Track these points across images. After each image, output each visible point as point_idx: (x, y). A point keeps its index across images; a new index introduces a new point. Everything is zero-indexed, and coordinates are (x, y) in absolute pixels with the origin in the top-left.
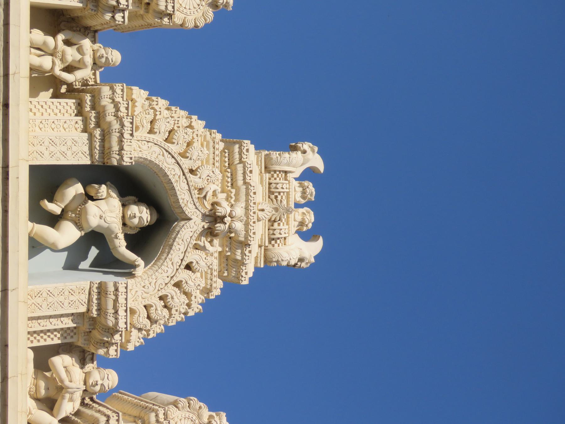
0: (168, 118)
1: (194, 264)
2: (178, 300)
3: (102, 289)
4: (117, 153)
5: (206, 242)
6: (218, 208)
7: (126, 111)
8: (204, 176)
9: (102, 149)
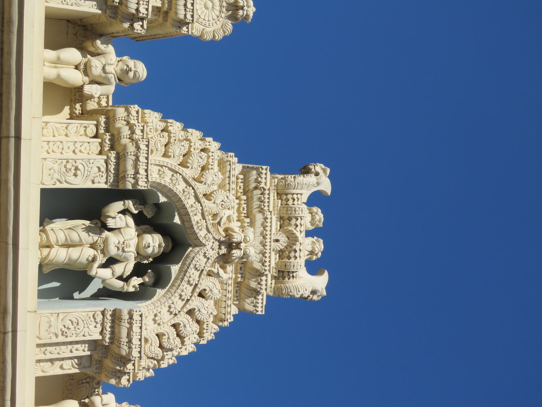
1: (207, 292)
3: (116, 316)
4: (132, 176)
5: (219, 269)
6: (234, 234)
7: (142, 134)
9: (116, 172)
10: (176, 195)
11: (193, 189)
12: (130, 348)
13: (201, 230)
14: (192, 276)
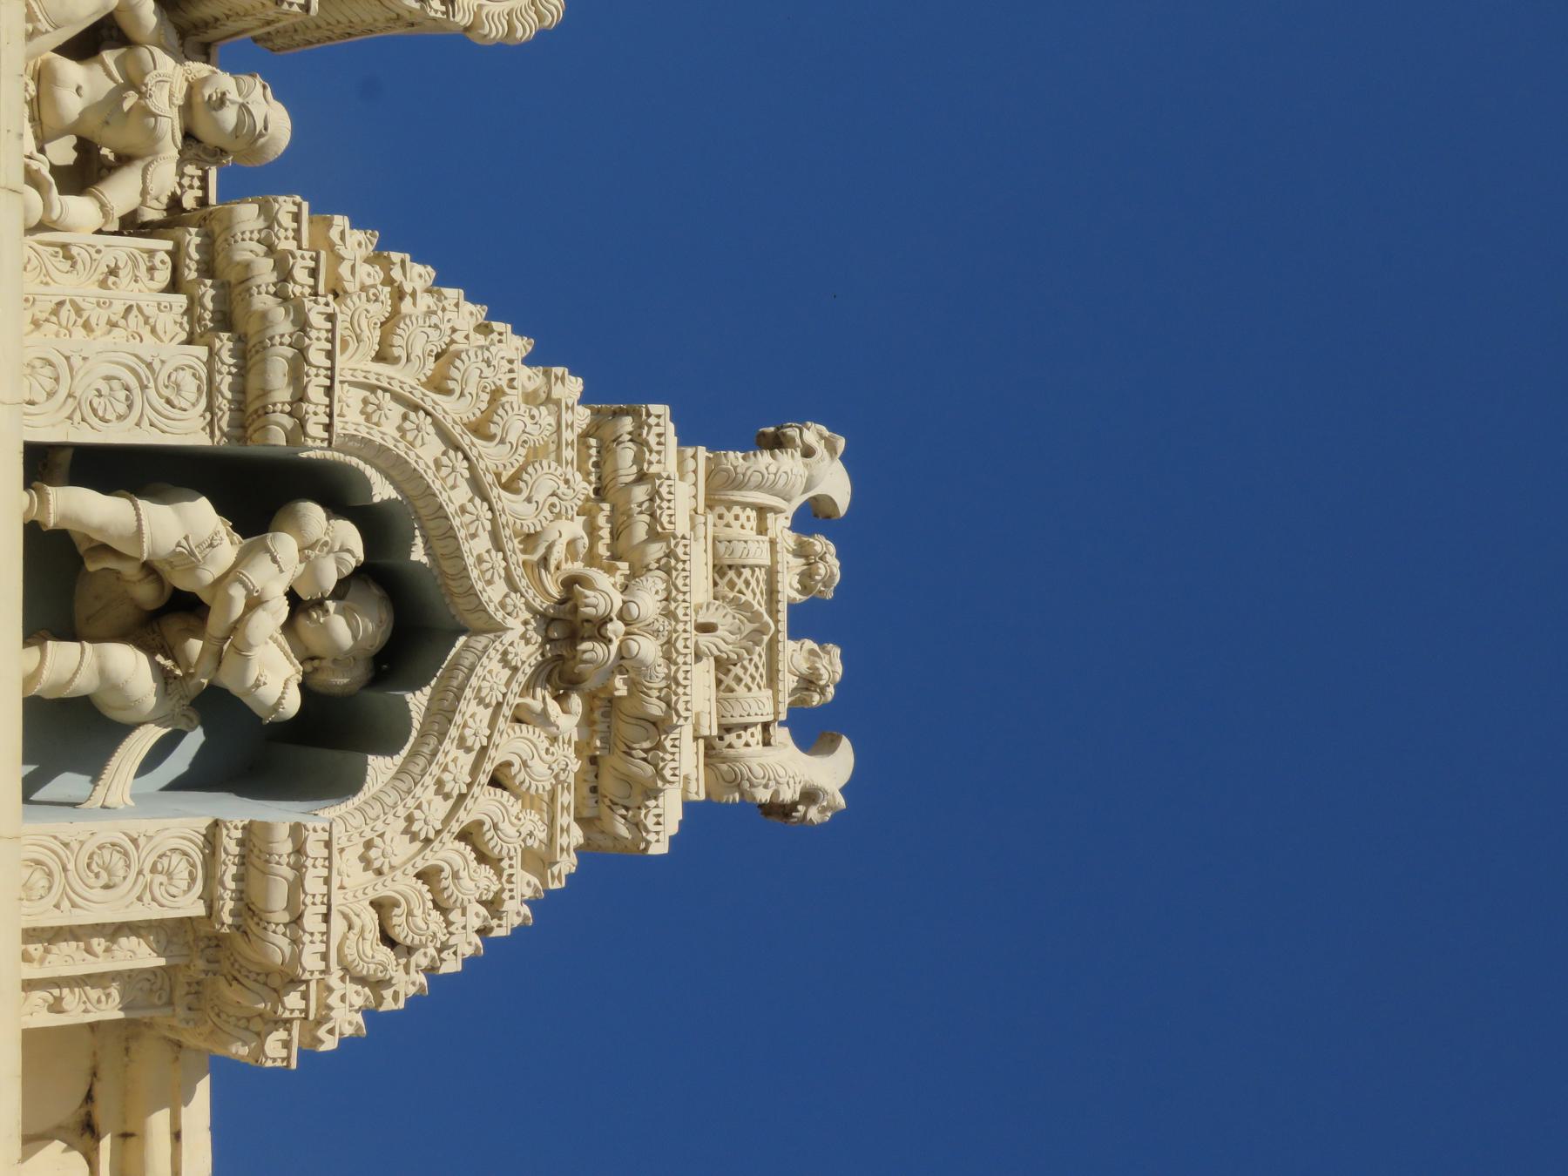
0: (435, 313)
1: (514, 770)
2: (475, 881)
4: (287, 408)
5: (549, 700)
6: (587, 592)
7: (311, 282)
8: (540, 496)
10: (416, 476)
11: (466, 457)
12: (295, 941)
13: (489, 582)
14: (470, 722)
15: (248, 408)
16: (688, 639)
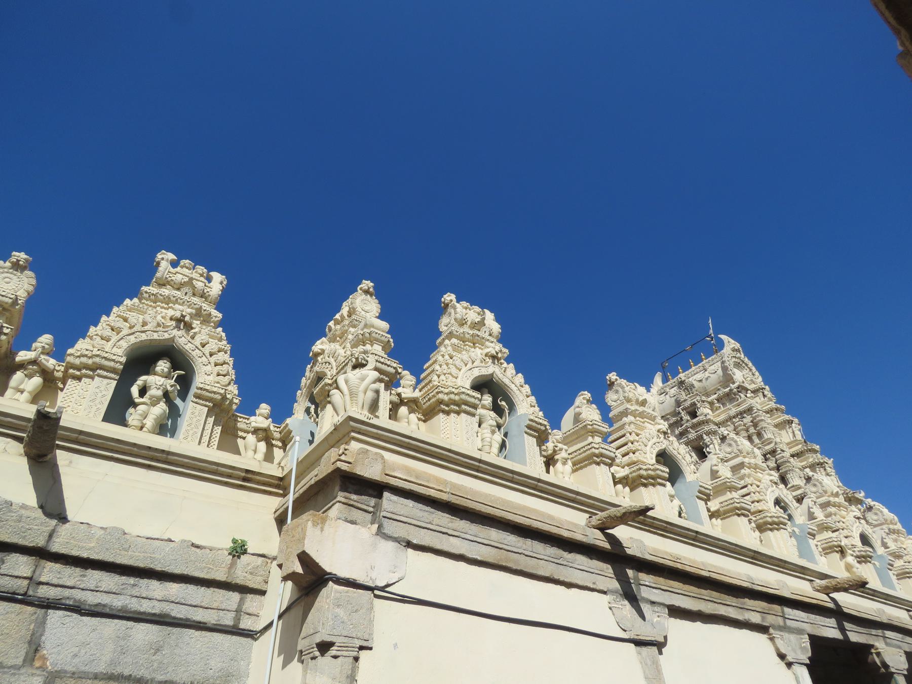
3: (197, 396)
15: (113, 371)
16: (186, 298)
